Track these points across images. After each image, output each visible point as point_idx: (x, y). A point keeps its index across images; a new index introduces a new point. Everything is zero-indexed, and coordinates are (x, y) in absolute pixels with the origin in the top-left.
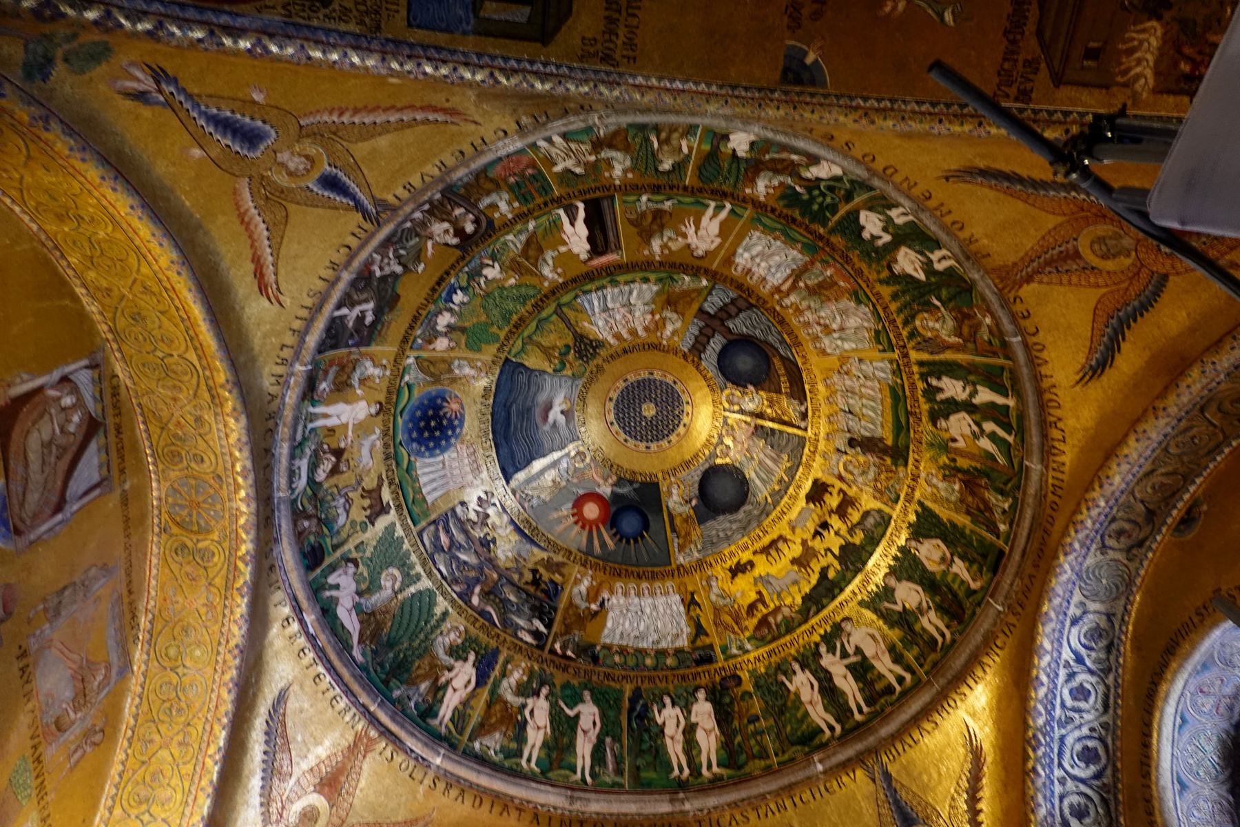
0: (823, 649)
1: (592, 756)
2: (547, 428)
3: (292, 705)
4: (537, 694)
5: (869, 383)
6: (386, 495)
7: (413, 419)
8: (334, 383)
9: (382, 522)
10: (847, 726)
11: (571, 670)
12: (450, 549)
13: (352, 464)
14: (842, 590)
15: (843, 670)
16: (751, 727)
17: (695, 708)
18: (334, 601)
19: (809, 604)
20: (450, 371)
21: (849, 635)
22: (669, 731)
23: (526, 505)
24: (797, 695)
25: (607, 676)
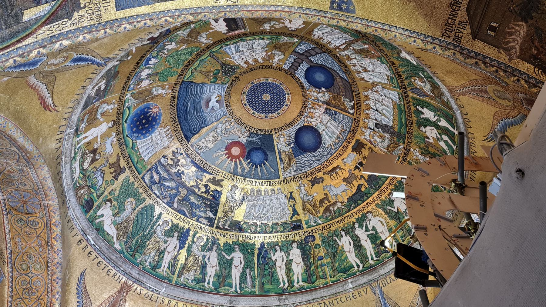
0: (357, 226)
1: (240, 278)
2: (209, 110)
4: (210, 249)
5: (387, 99)
6: (123, 163)
7: (132, 122)
8: (88, 122)
10: (365, 266)
12: (160, 181)
13: (102, 154)
14: (368, 198)
15: (366, 238)
16: (319, 262)
17: (292, 252)
18: (102, 223)
19: (351, 202)
20: (151, 94)
21: (370, 220)
22: (278, 264)
23: (199, 152)
24: (343, 248)
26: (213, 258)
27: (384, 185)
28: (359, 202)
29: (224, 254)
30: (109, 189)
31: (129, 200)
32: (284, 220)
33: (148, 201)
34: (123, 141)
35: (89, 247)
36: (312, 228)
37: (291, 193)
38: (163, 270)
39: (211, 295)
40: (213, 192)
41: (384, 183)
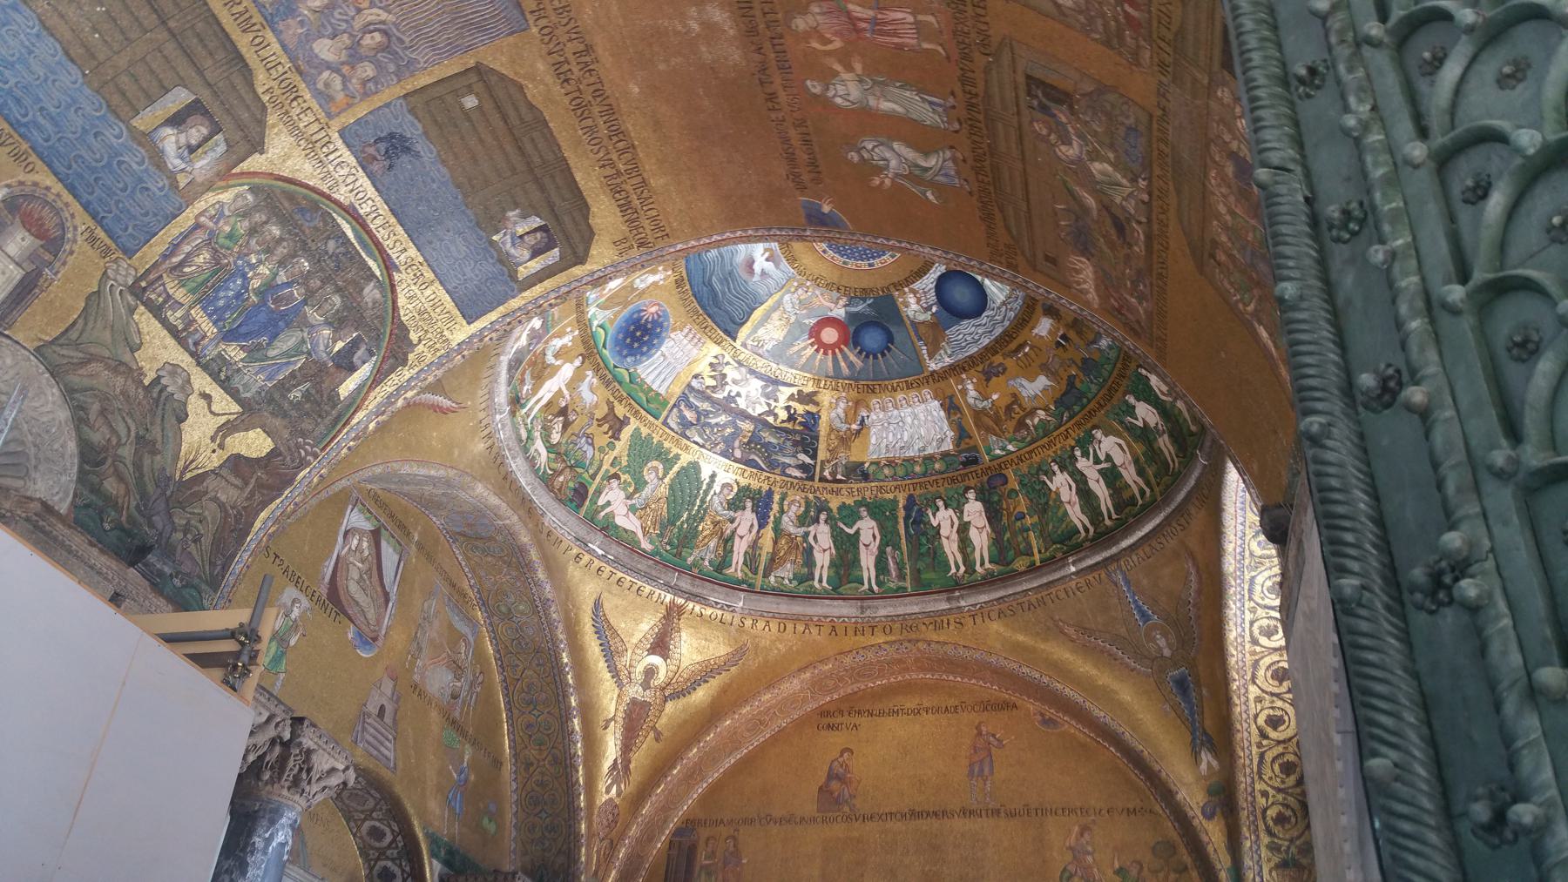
0: (1078, 453)
2: (756, 278)
3: (607, 606)
4: (816, 521)
6: (620, 411)
7: (617, 342)
8: (533, 377)
9: (626, 433)
11: (844, 491)
12: (698, 420)
15: (1097, 475)
16: (1018, 524)
18: (611, 515)
22: (944, 532)
23: (760, 351)
24: (1058, 494)
26: (822, 535)
27: (1111, 379)
29: (842, 526)
30: (608, 459)
31: (649, 465)
33: (685, 459)
34: (610, 376)
35: (596, 561)
36: (998, 461)
38: (737, 567)
39: (827, 602)
40: (802, 416)
41: (1111, 373)
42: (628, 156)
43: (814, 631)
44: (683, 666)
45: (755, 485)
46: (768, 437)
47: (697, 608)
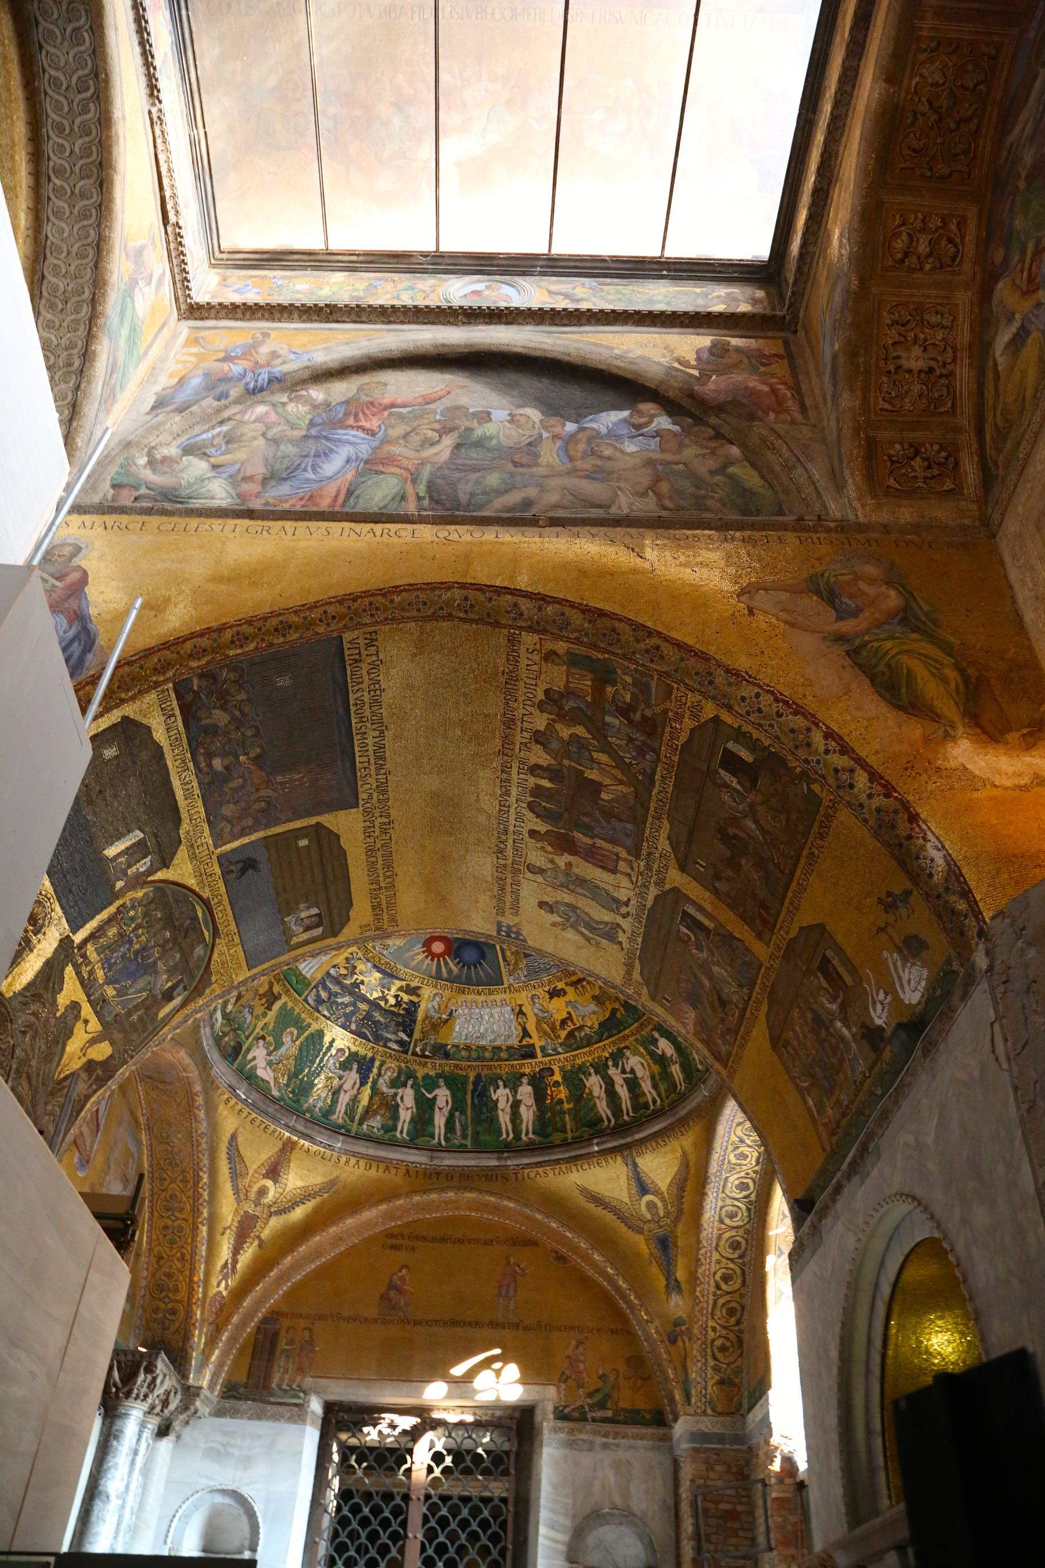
1: (446, 1126)
3: (240, 1139)
4: (405, 1085)
12: (329, 998)
14: (625, 1029)
15: (621, 1082)
16: (558, 1107)
17: (521, 1089)
22: (501, 1105)
25: (456, 1066)
26: (407, 1097)
28: (614, 1031)
29: (424, 1091)
30: (261, 1024)
32: (510, 1043)
37: (520, 1006)
39: (405, 1150)
40: (406, 1003)
42: (390, 880)
43: (393, 1171)
44: (287, 1190)
45: (362, 1052)
46: (377, 1016)
47: (307, 1144)
